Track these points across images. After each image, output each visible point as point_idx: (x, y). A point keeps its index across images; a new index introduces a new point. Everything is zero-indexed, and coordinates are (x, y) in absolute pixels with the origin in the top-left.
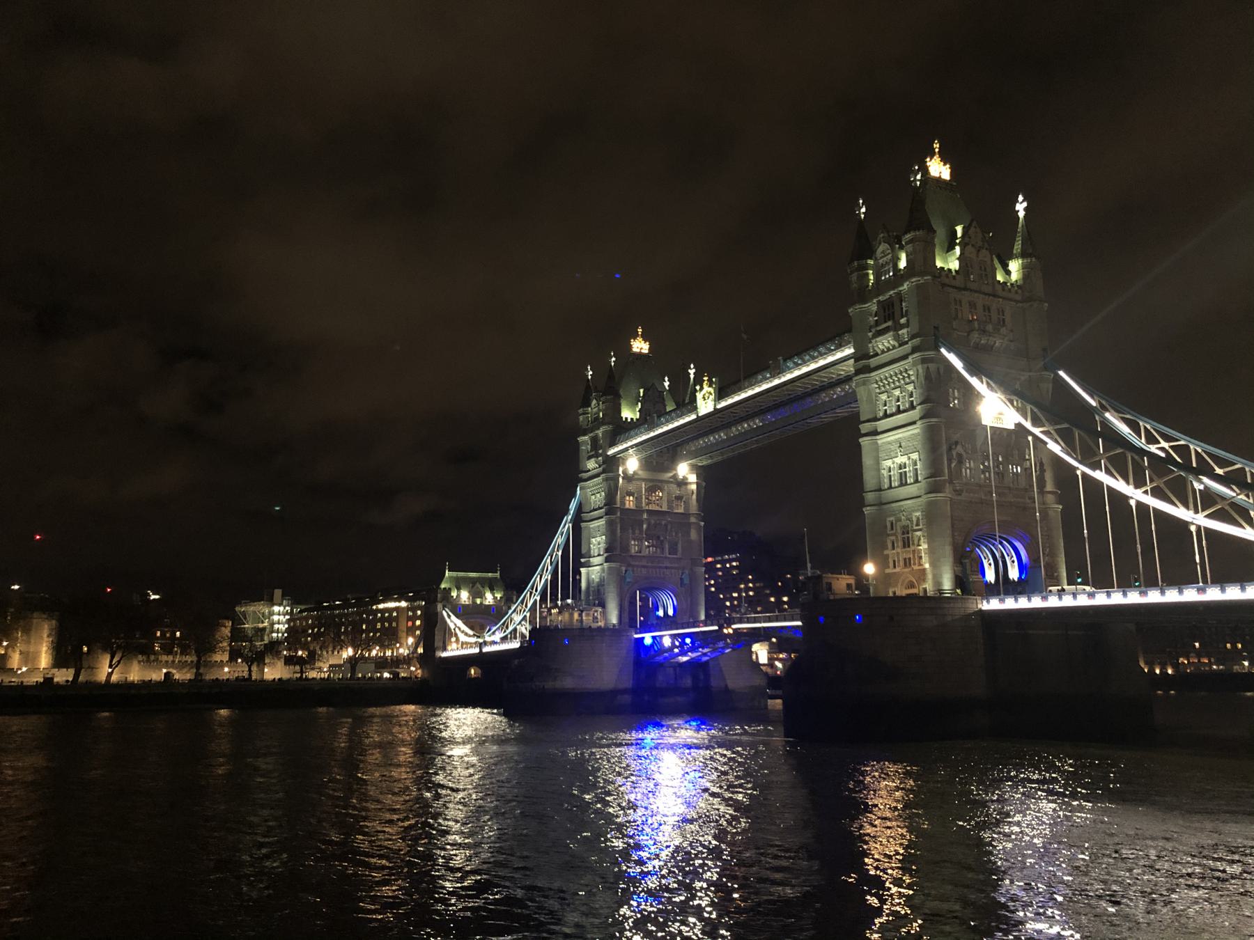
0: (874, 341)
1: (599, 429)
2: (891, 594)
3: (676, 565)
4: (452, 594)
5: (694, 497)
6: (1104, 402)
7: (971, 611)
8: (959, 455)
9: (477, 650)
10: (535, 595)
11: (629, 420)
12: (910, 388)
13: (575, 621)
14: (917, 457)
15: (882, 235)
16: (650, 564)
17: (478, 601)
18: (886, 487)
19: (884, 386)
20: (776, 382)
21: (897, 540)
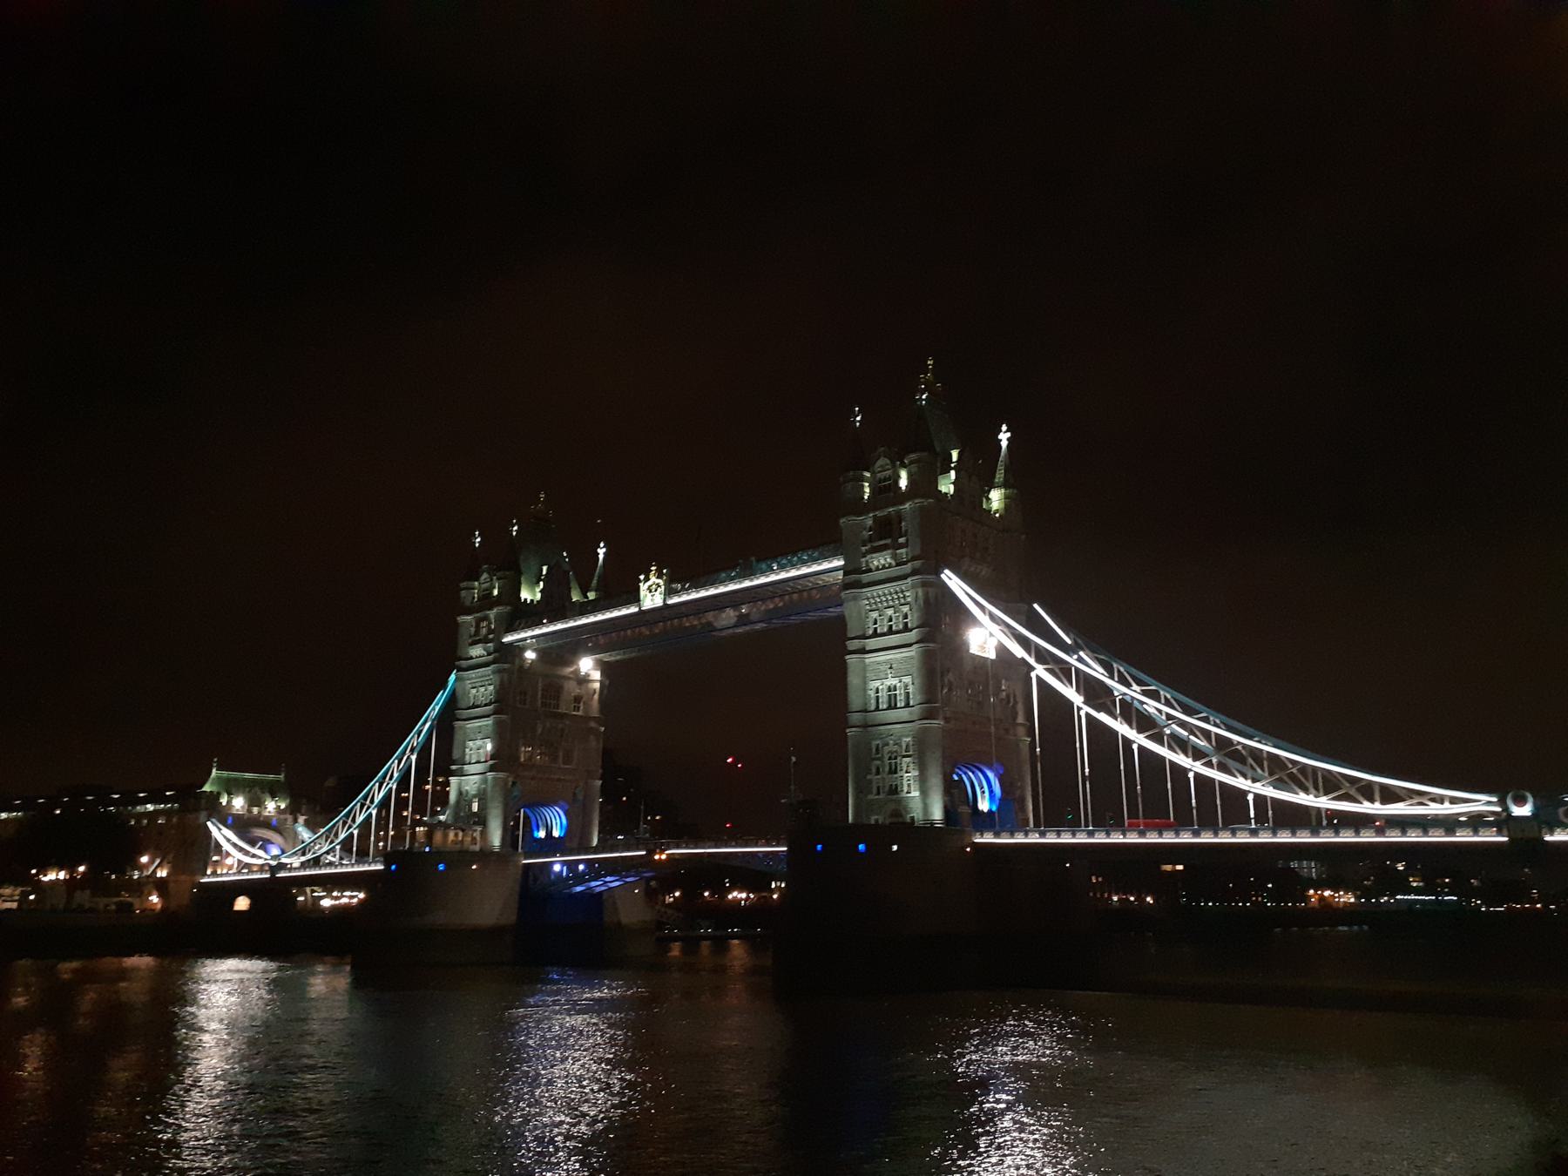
1: (490, 609)
2: (873, 822)
5: (596, 696)
6: (1080, 641)
8: (950, 683)
10: (369, 808)
12: (905, 609)
14: (910, 680)
15: (882, 449)
17: (255, 810)
18: (873, 708)
20: (747, 584)
21: (884, 766)
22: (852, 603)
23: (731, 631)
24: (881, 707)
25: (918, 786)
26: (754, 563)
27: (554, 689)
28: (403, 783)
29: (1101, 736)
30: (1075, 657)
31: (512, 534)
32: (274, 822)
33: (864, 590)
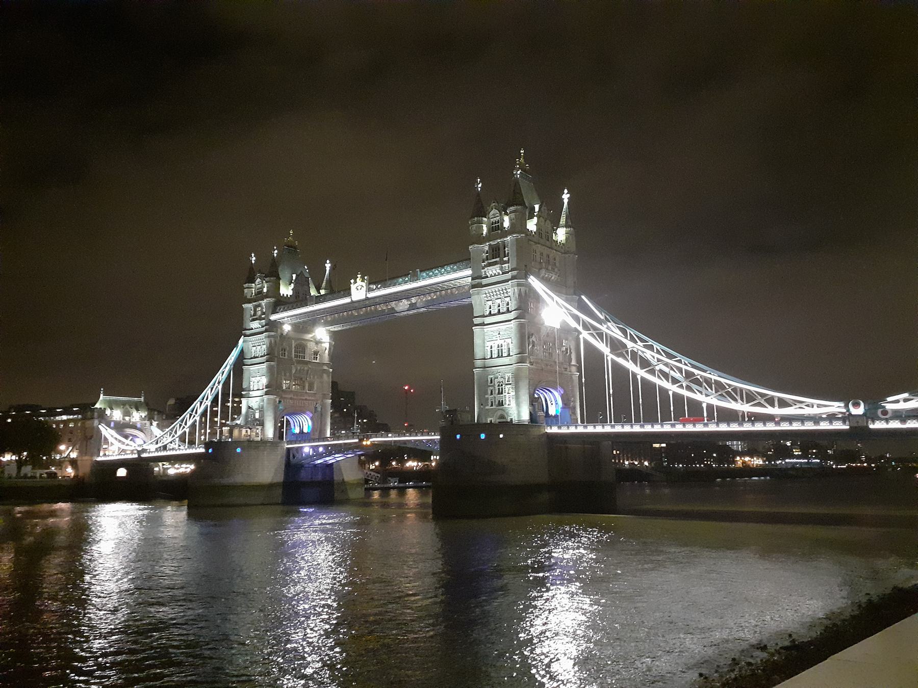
1: (263, 300)
2: (489, 422)
3: (312, 398)
5: (327, 352)
6: (607, 317)
7: (542, 433)
8: (533, 342)
9: (136, 456)
10: (194, 416)
11: (285, 296)
12: (508, 299)
13: (243, 435)
15: (494, 204)
16: (295, 397)
17: (127, 418)
21: (495, 390)
22: (476, 296)
23: (405, 313)
25: (514, 401)
26: (419, 273)
27: (301, 348)
28: (215, 401)
29: (620, 373)
30: (606, 326)
32: (139, 425)
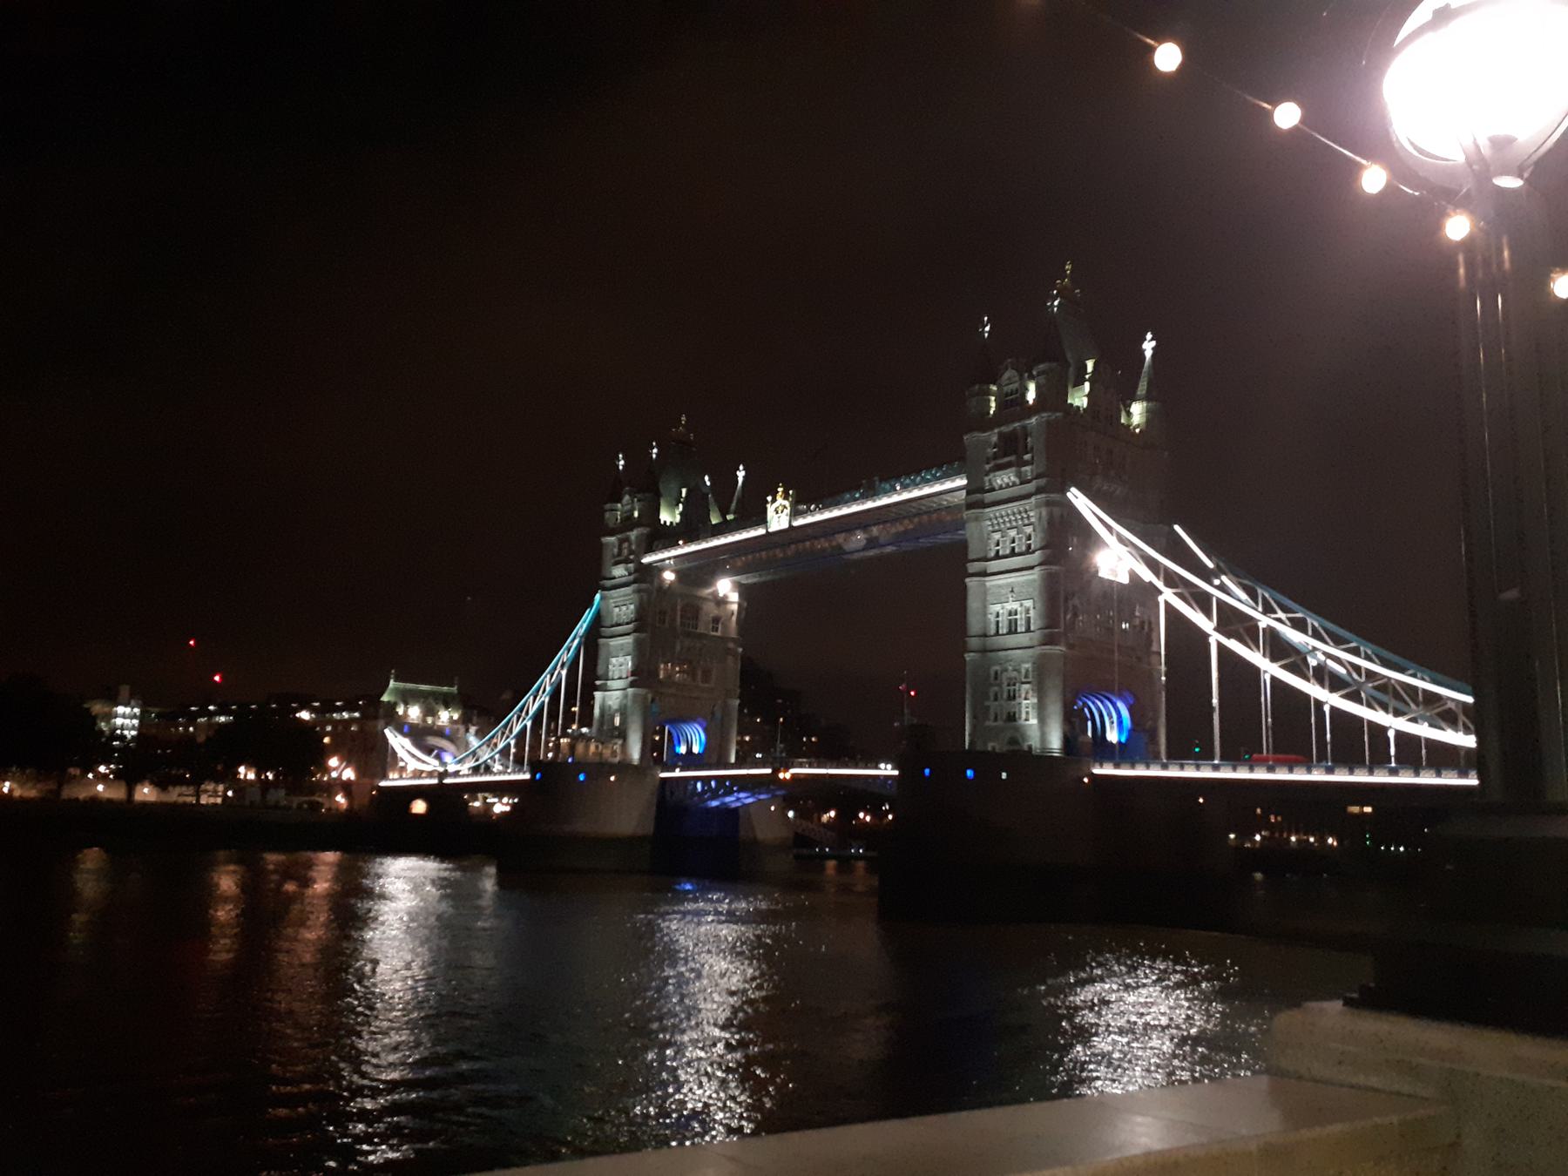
0: (991, 475)
1: (632, 530)
2: (990, 749)
4: (397, 710)
5: (734, 618)
6: (1222, 565)
8: (1075, 607)
9: (435, 781)
10: (524, 719)
11: (668, 524)
12: (1029, 530)
13: (590, 754)
15: (1009, 360)
17: (430, 720)
18: (993, 632)
19: (998, 524)
20: (870, 505)
23: (862, 554)
24: (1000, 632)
26: (877, 483)
27: (693, 610)
28: (555, 695)
31: (652, 457)
32: (447, 731)
33: (987, 510)
